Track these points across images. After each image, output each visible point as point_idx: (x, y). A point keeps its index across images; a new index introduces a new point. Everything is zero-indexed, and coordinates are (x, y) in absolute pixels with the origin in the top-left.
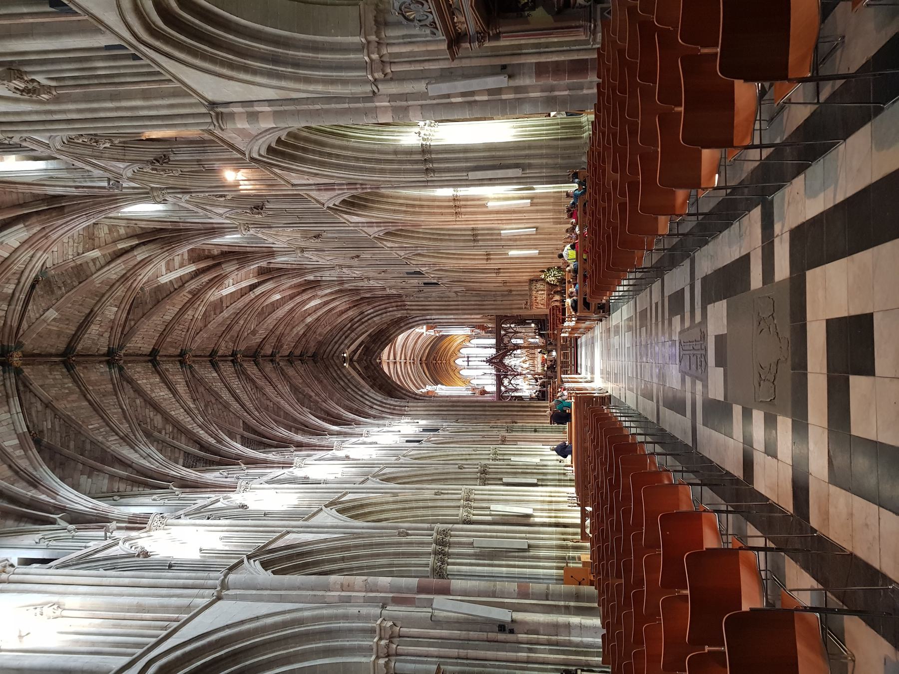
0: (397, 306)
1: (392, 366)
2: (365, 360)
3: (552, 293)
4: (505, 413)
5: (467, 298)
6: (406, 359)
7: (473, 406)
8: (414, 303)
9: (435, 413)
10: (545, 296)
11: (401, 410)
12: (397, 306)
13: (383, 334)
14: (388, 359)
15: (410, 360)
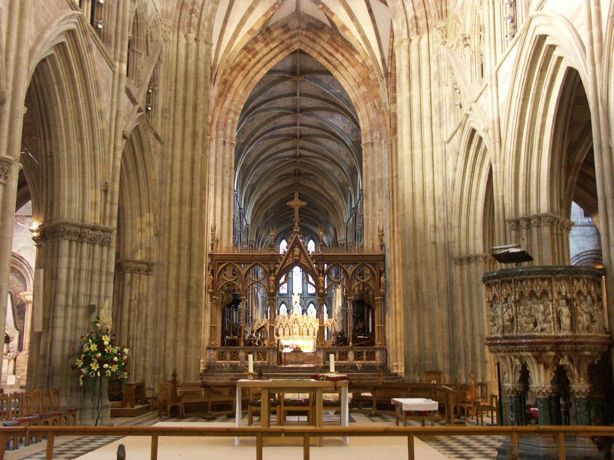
0: (416, 18)
1: (287, 102)
2: (299, 27)
3: (564, 362)
4: (175, 250)
5: (438, 166)
6: (302, 137)
7: (192, 178)
8: (424, 52)
9: (180, 94)
10: (551, 331)
11: (190, 25)
12: (416, 18)
13: (347, 55)
14: (301, 95)
15: (302, 148)
